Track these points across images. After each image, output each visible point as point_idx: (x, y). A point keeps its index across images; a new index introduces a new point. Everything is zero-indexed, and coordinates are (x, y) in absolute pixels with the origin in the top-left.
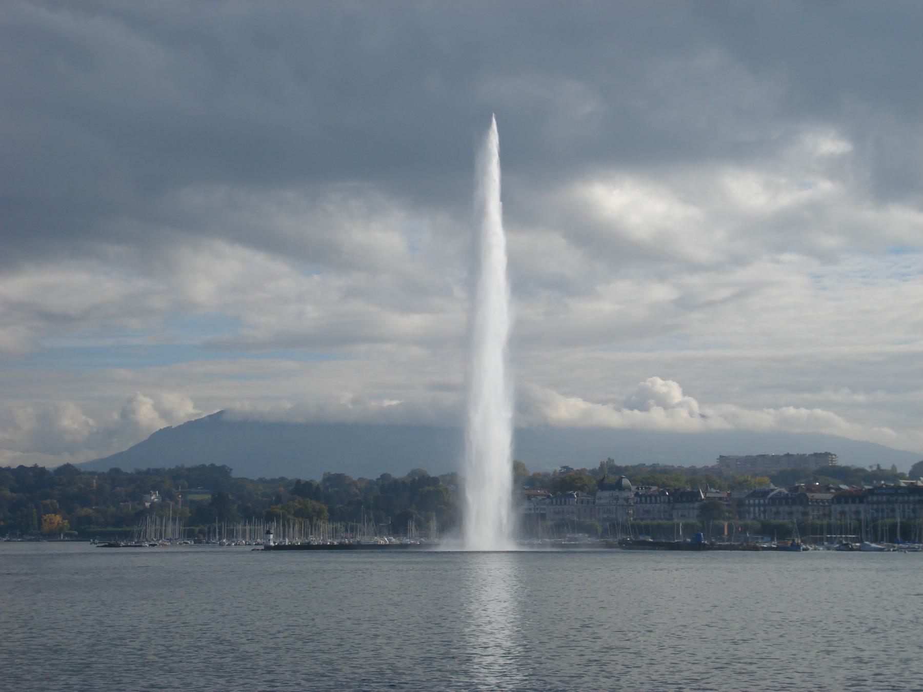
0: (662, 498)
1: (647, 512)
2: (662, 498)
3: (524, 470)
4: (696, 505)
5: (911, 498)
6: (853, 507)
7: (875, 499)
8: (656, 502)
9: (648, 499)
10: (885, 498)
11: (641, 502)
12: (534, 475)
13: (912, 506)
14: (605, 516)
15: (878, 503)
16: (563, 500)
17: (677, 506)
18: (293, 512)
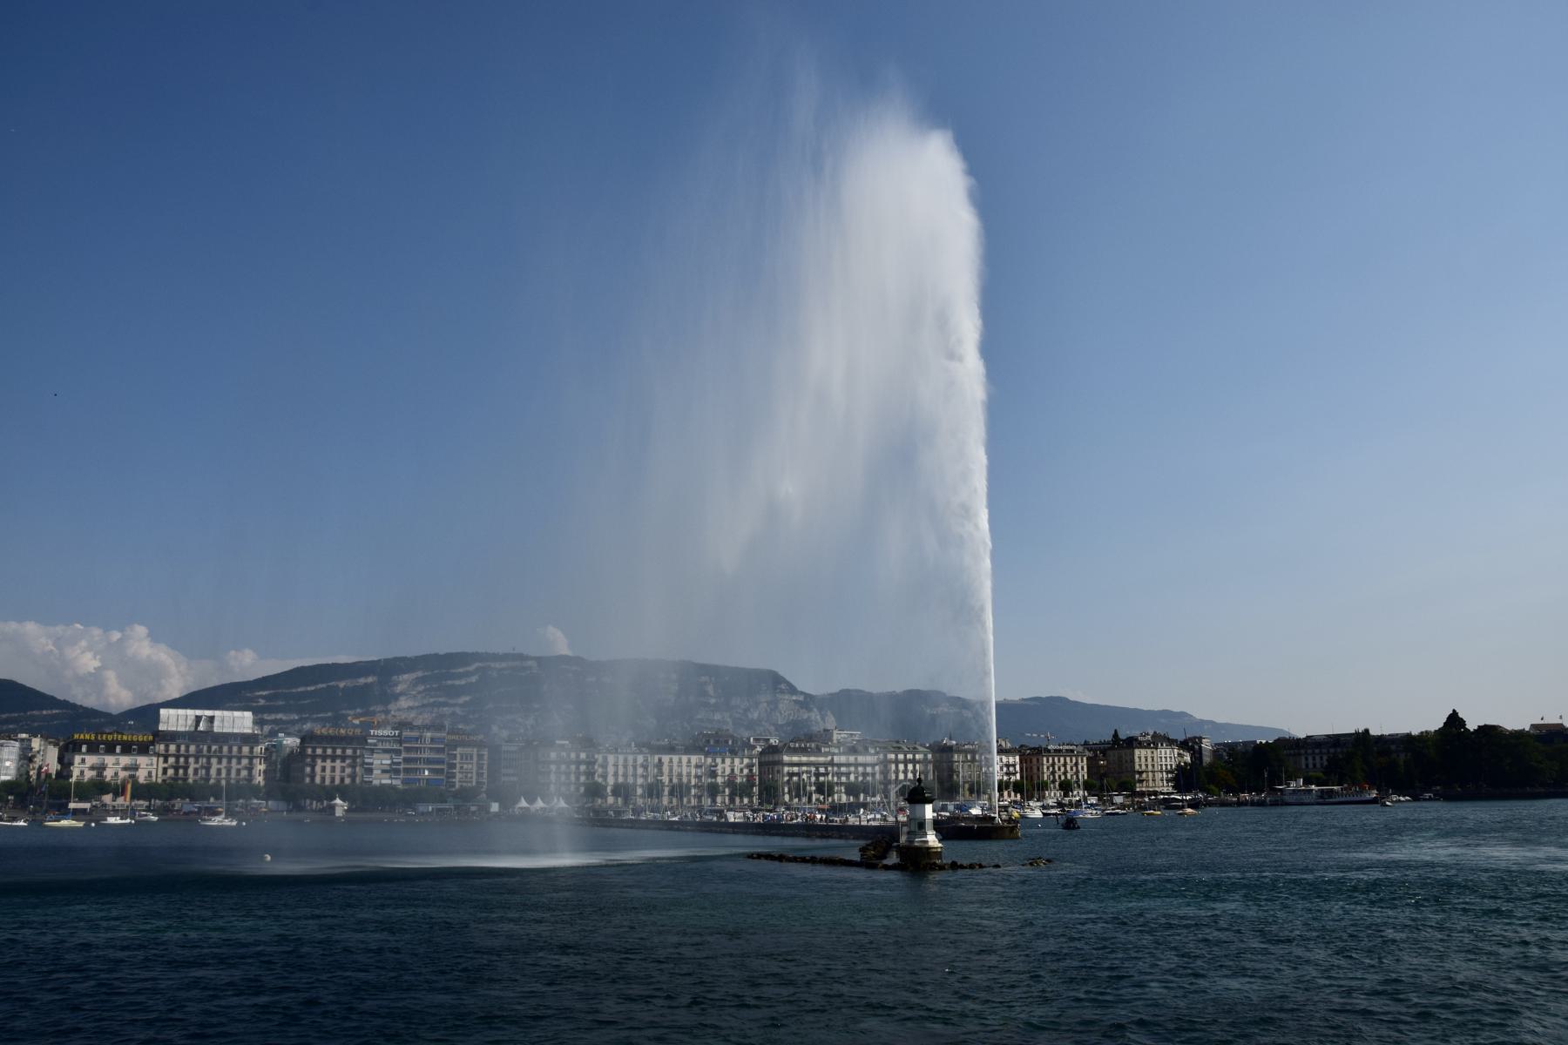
6: (125, 760)
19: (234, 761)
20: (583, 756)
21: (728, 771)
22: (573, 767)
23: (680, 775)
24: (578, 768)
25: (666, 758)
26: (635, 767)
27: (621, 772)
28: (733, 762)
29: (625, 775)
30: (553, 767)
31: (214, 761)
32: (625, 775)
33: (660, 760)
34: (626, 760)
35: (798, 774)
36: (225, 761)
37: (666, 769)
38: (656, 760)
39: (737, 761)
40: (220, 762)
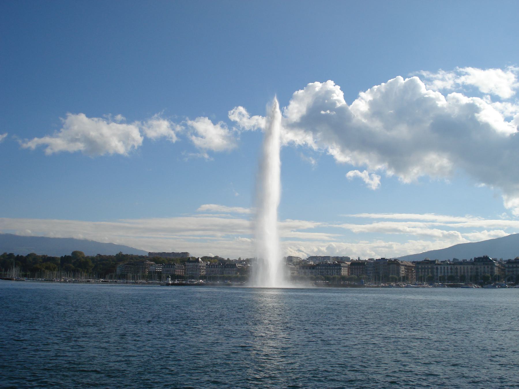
0: (220, 266)
1: (213, 271)
2: (220, 266)
3: (83, 255)
4: (235, 269)
5: (336, 267)
7: (320, 267)
8: (217, 267)
9: (213, 266)
10: (324, 267)
11: (209, 267)
12: (87, 257)
13: (336, 270)
14: (191, 272)
15: (321, 269)
16: (168, 266)
17: (226, 269)
18: (45, 267)
19: (333, 270)
20: (430, 267)
21: (483, 271)
22: (426, 270)
23: (464, 272)
24: (428, 271)
25: (459, 267)
26: (448, 270)
27: (443, 271)
28: (484, 267)
29: (444, 272)
30: (420, 270)
31: (329, 270)
32: (444, 272)
33: (457, 267)
34: (444, 268)
35: (513, 271)
36: (331, 271)
37: (459, 271)
38: (455, 267)
39: (486, 266)
40: (330, 271)
